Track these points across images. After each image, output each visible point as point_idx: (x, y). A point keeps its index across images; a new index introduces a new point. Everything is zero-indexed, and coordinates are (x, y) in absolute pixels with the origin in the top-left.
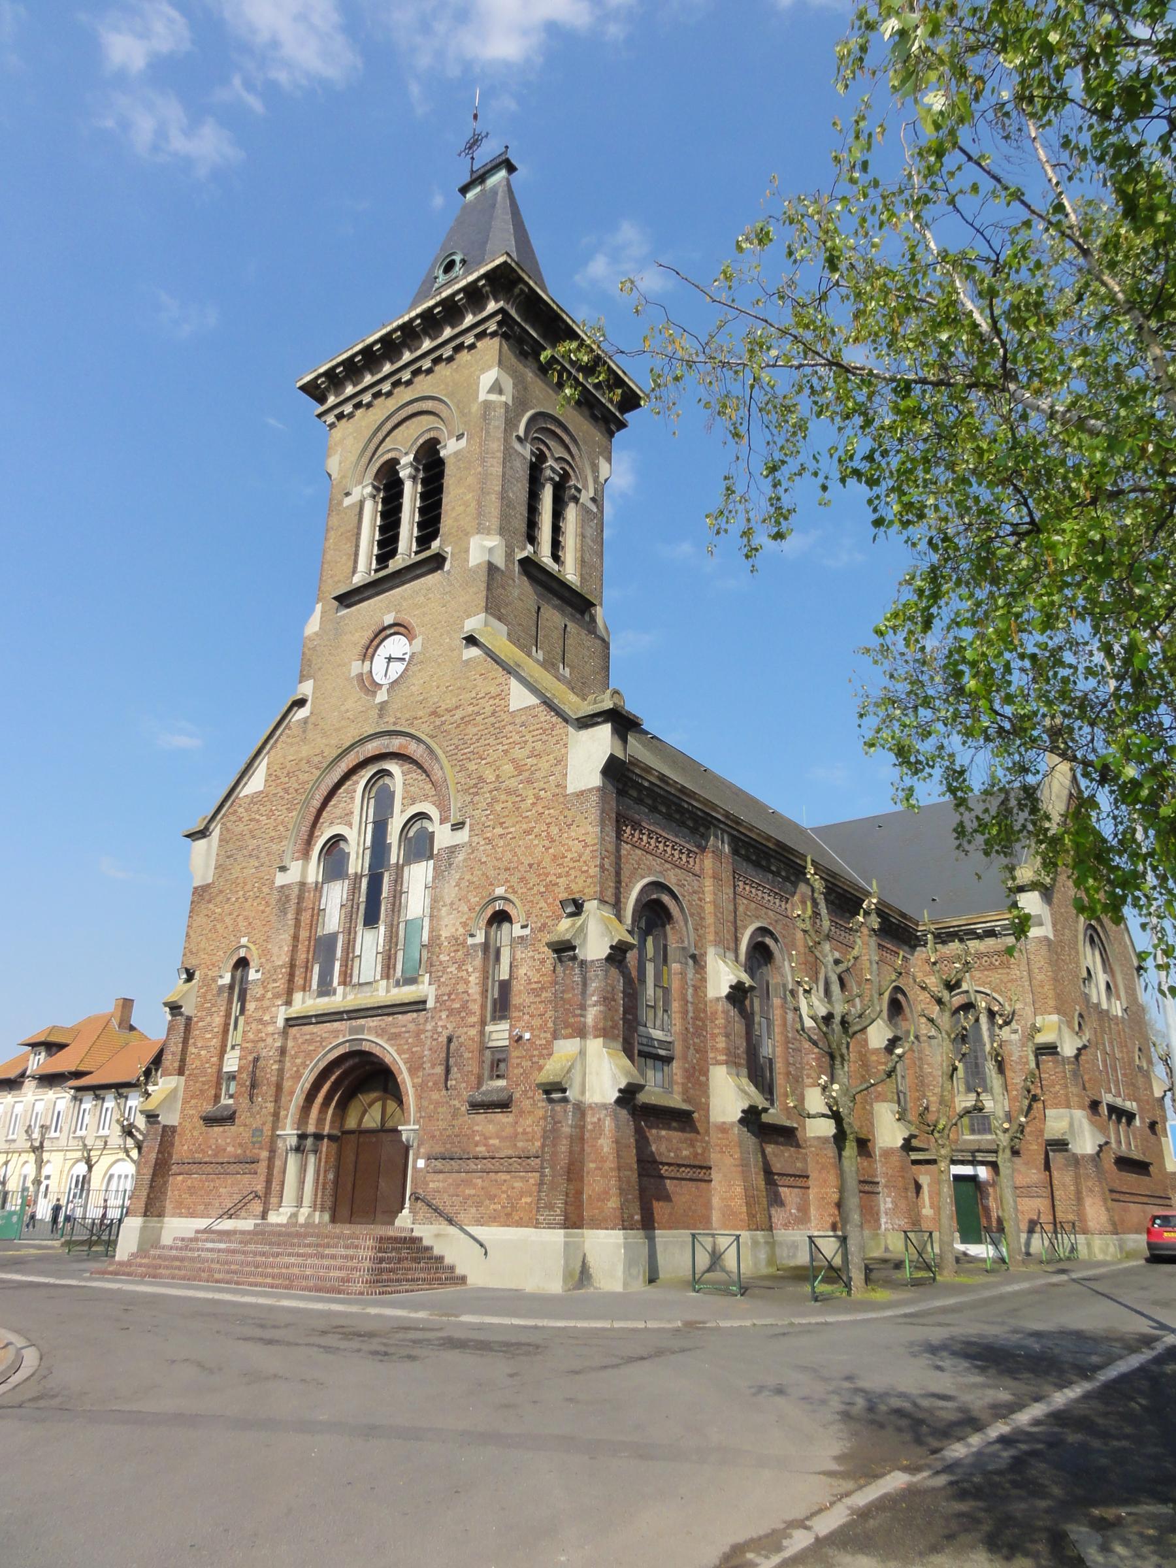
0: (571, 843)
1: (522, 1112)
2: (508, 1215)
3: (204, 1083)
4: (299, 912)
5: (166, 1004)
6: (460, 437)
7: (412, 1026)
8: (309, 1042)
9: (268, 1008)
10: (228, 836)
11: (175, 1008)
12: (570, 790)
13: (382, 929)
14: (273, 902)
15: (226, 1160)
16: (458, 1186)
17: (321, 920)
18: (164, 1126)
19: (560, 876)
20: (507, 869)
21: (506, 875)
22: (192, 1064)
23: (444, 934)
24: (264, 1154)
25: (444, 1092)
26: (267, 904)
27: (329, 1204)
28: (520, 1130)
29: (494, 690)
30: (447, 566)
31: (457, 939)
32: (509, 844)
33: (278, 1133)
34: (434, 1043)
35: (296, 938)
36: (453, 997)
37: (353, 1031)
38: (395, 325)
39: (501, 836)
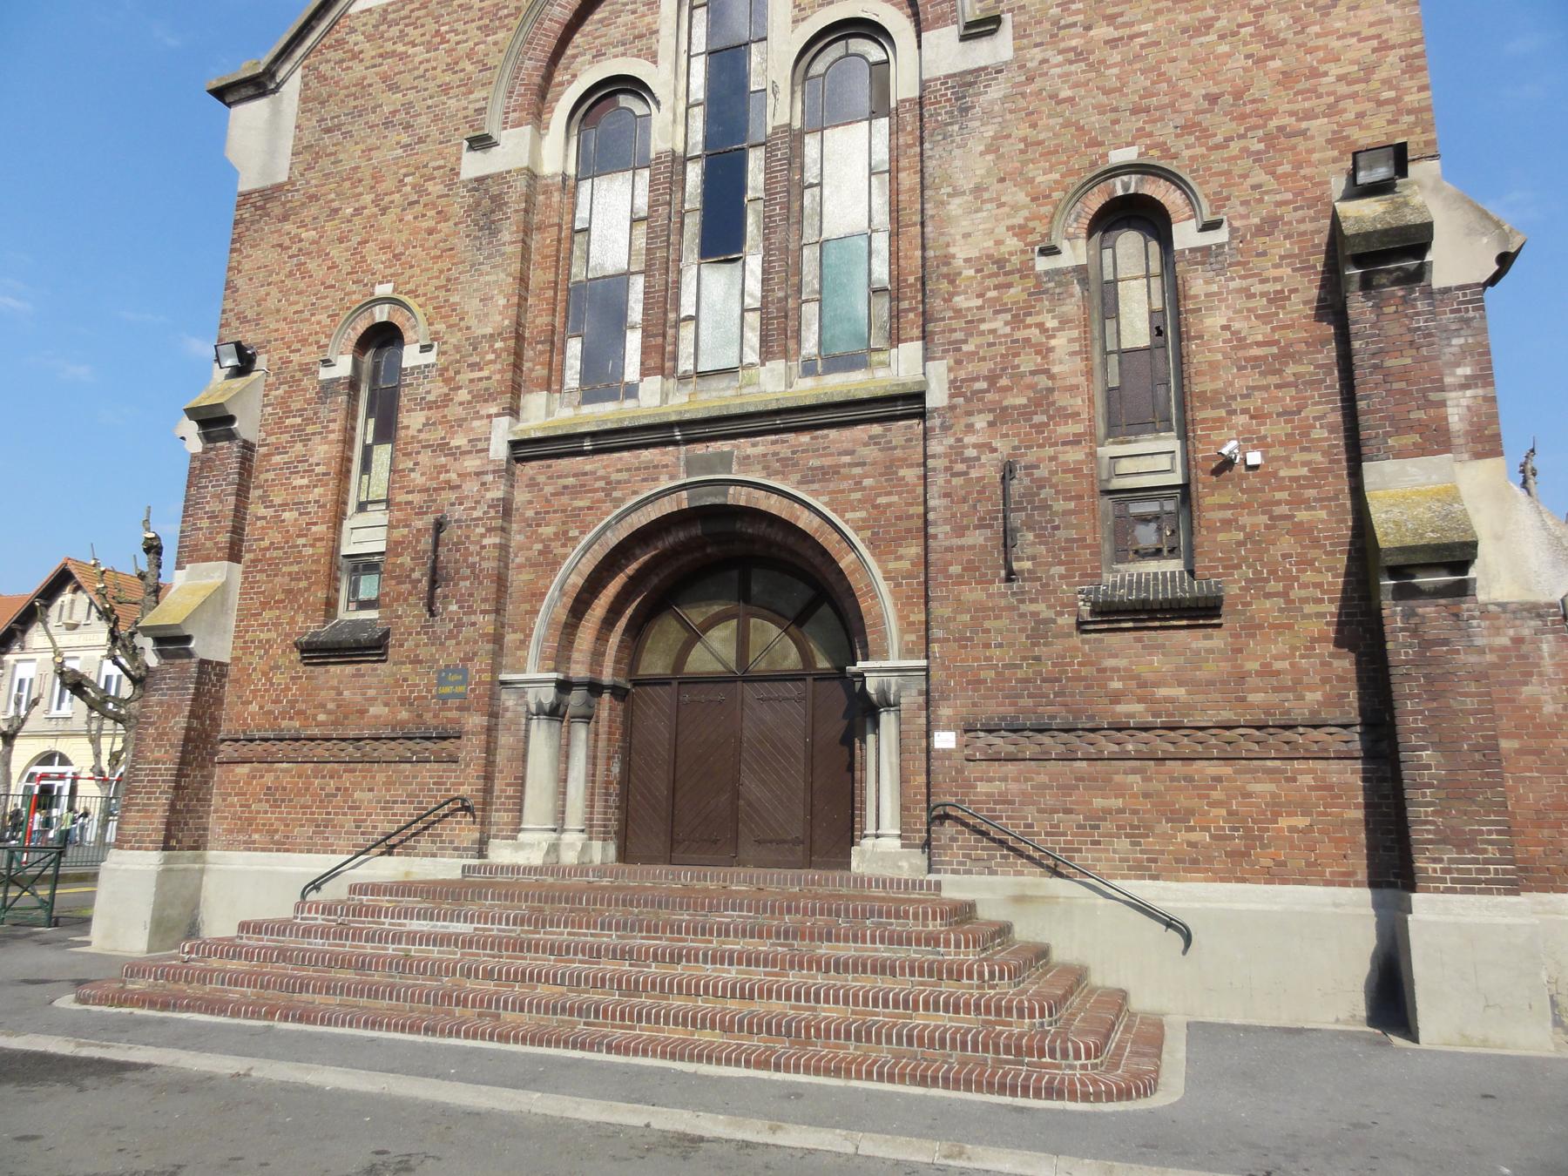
0: (1335, 44)
1: (1252, 628)
2: (1237, 855)
3: (294, 577)
4: (527, 230)
5: (192, 413)
7: (871, 453)
8: (573, 491)
9: (460, 422)
10: (324, 91)
11: (214, 422)
13: (754, 262)
14: (457, 210)
15: (366, 733)
16: (1067, 789)
17: (577, 252)
18: (203, 662)
19: (1309, 115)
20: (1135, 111)
21: (1139, 122)
22: (260, 536)
23: (961, 252)
24: (475, 721)
25: (999, 587)
26: (442, 216)
27: (614, 825)
28: (1253, 666)
31: (1000, 263)
32: (1137, 57)
33: (504, 677)
34: (956, 481)
35: (523, 280)
36: (1004, 382)
39: (1112, 43)
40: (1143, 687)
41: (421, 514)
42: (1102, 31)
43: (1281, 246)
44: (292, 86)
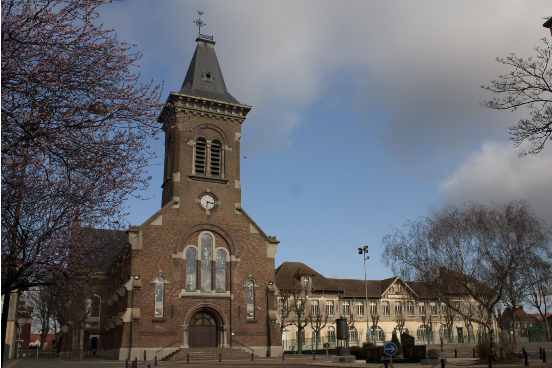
6: (230, 147)
12: (268, 257)
23: (235, 283)
29: (245, 226)
30: (228, 184)
37: (204, 302)
38: (213, 101)
40: (250, 329)
41: (169, 304)
42: (249, 261)
43: (263, 288)
44: (141, 233)
